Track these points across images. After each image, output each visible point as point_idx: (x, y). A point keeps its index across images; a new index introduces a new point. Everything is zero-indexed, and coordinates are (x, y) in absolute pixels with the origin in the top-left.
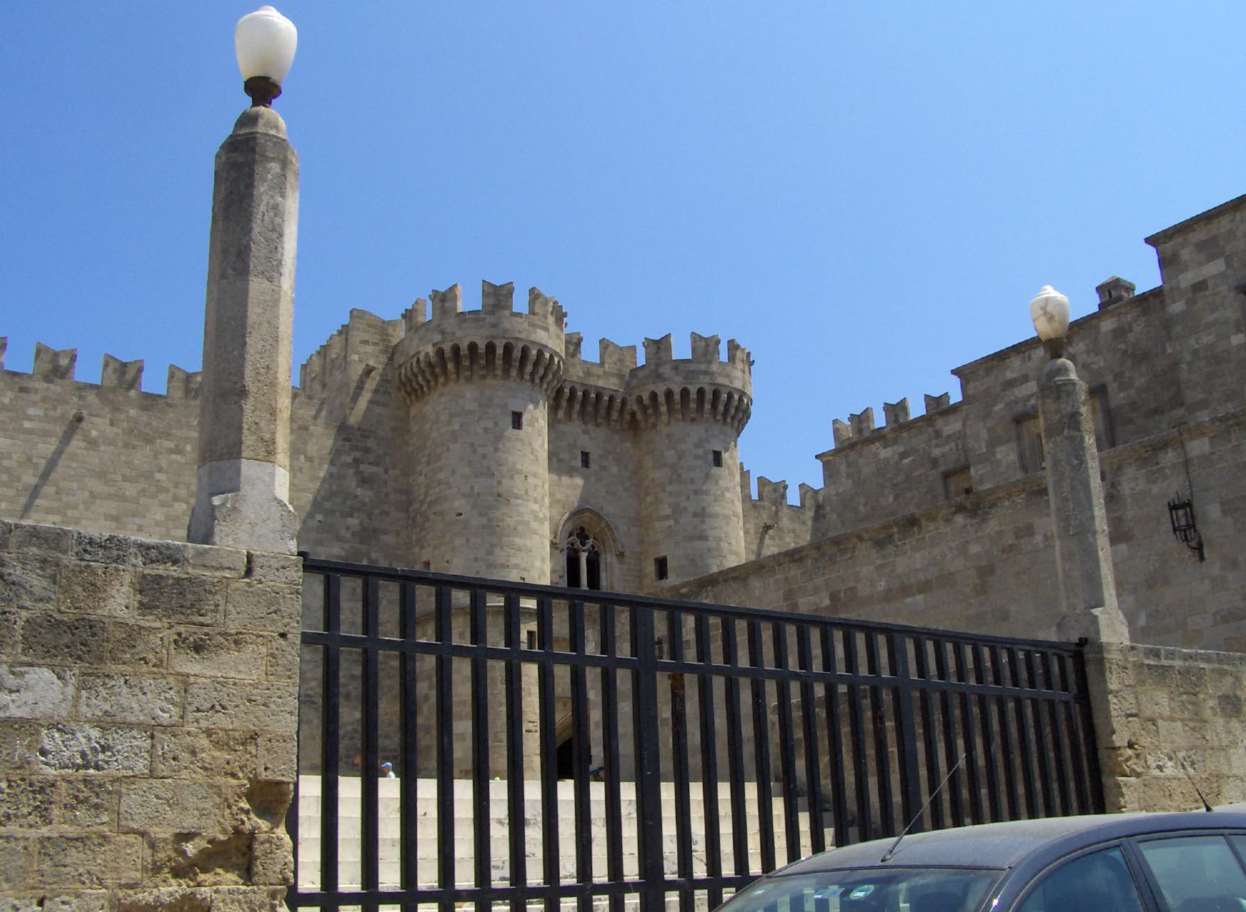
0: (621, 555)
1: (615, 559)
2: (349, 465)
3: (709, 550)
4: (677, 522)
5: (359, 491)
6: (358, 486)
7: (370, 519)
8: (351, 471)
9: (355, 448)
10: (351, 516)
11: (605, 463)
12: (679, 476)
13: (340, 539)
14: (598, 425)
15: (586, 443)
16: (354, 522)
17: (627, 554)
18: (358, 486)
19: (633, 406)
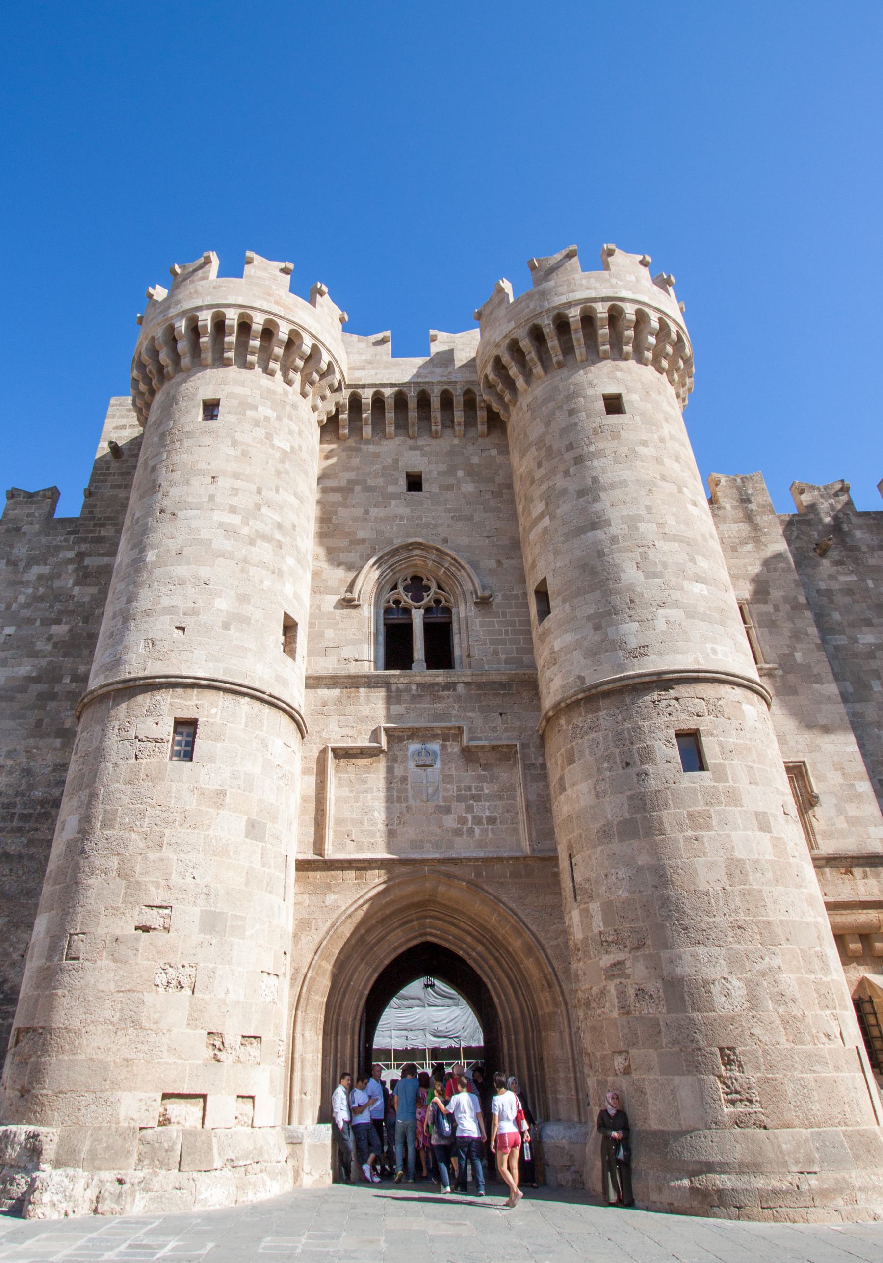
0: (484, 603)
1: (473, 610)
2: (70, 561)
3: (614, 540)
4: (553, 517)
5: (77, 589)
6: (76, 584)
7: (86, 620)
8: (71, 568)
9: (85, 540)
10: (58, 622)
11: (451, 481)
12: (550, 449)
13: (34, 654)
14: (435, 436)
15: (415, 461)
16: (60, 630)
17: (498, 599)
18: (76, 584)
19: (484, 396)
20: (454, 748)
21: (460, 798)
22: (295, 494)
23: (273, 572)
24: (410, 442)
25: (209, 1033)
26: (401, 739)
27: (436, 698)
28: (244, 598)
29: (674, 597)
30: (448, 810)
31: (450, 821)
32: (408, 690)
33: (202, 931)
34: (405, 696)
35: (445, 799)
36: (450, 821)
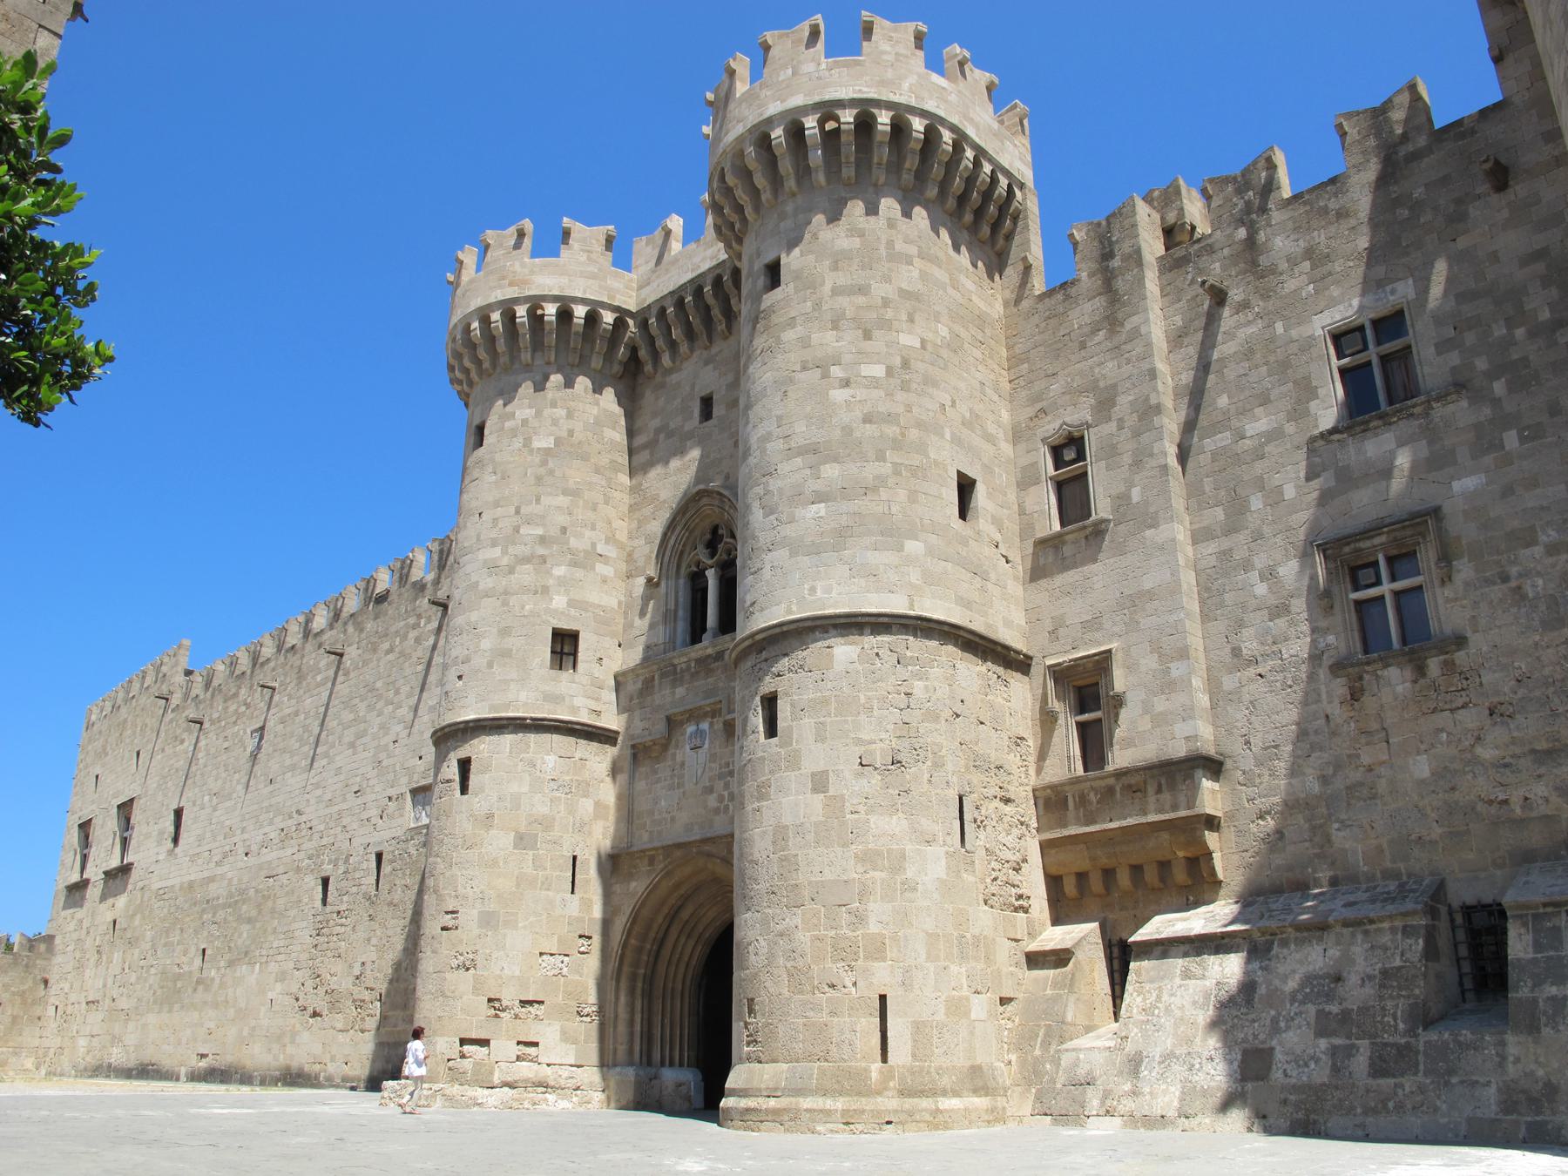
20: (719, 726)
21: (721, 776)
22: (565, 492)
23: (536, 592)
24: (705, 353)
25: (490, 1000)
26: (682, 723)
27: (709, 672)
28: (505, 632)
29: (783, 534)
30: (709, 790)
31: (712, 801)
32: (689, 668)
33: (480, 927)
34: (687, 677)
35: (711, 779)
36: (712, 801)
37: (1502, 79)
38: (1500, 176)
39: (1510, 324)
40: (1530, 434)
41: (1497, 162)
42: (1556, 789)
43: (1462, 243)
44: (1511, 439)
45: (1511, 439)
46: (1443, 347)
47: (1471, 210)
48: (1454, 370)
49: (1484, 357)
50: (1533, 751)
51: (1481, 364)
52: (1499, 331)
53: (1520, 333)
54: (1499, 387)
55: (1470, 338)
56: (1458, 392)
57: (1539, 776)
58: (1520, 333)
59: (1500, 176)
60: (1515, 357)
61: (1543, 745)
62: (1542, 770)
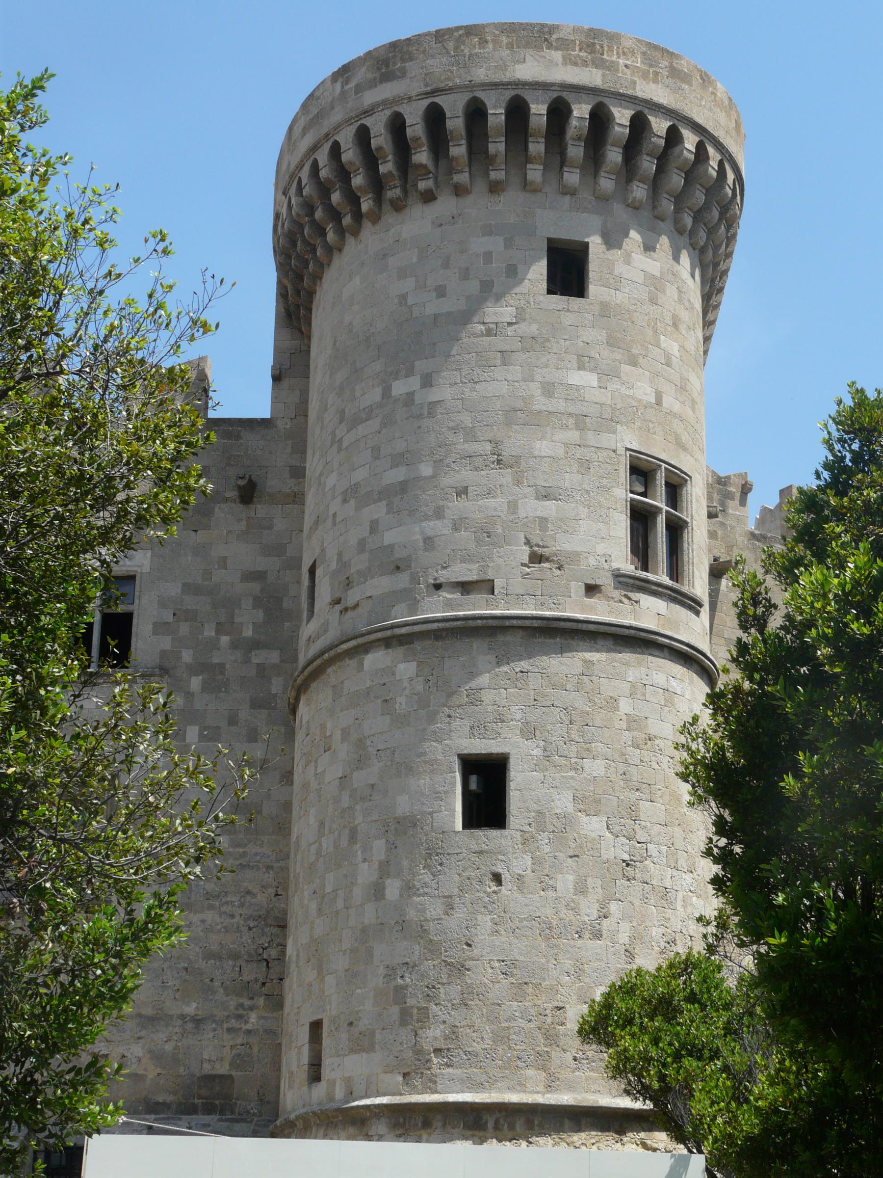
37: (275, 400)
38: (248, 493)
39: (220, 629)
40: (210, 735)
41: (250, 480)
42: (150, 1051)
43: (201, 537)
44: (192, 733)
45: (192, 733)
46: (160, 628)
47: (217, 509)
48: (163, 653)
49: (191, 652)
50: (139, 1015)
51: (187, 656)
52: (209, 632)
53: (225, 640)
54: (195, 683)
55: (184, 629)
56: (161, 676)
57: (139, 1038)
58: (225, 640)
59: (248, 493)
60: (216, 660)
61: (148, 1011)
62: (143, 1033)
